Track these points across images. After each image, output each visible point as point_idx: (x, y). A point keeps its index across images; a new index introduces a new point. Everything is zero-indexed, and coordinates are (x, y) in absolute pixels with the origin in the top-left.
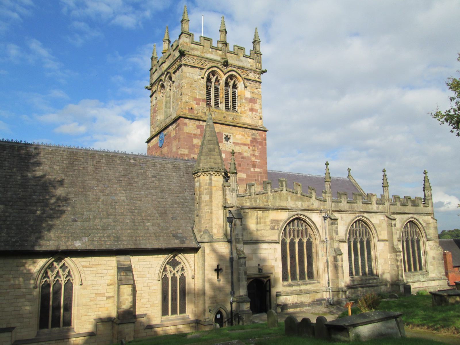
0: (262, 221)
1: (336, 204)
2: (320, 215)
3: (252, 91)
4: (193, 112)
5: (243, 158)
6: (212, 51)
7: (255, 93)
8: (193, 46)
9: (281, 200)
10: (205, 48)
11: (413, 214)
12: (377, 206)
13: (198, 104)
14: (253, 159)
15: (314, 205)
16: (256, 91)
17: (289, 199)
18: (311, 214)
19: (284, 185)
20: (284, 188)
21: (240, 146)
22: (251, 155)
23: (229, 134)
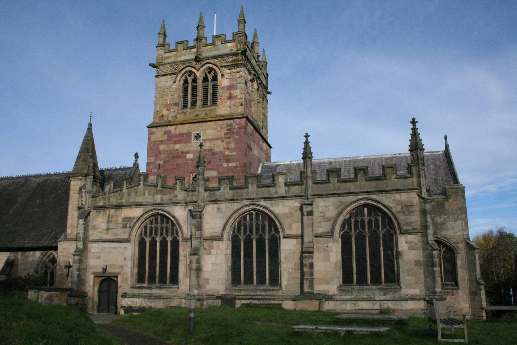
0: (113, 219)
1: (212, 193)
5: (214, 154)
6: (186, 52)
8: (166, 55)
9: (136, 195)
10: (179, 52)
11: (369, 193)
12: (287, 188)
13: (168, 110)
14: (227, 153)
17: (147, 193)
18: (173, 207)
19: (142, 180)
20: (142, 183)
21: (211, 142)
22: (224, 149)
23: (199, 132)
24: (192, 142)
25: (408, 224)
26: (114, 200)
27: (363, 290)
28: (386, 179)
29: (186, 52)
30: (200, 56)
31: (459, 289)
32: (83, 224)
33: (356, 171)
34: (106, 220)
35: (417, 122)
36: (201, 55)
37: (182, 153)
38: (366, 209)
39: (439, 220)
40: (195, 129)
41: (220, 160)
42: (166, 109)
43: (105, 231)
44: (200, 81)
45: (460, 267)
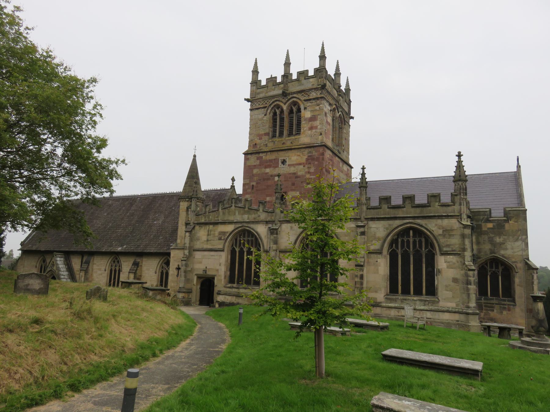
0: (212, 233)
2: (266, 225)
3: (312, 109)
4: (256, 147)
5: (297, 177)
7: (316, 110)
10: (269, 88)
11: (414, 218)
13: (260, 139)
14: (308, 176)
15: (261, 216)
16: (317, 108)
17: (237, 213)
18: (257, 225)
19: (234, 202)
20: (233, 205)
22: (306, 173)
23: (285, 158)
24: (280, 167)
25: (448, 246)
26: (212, 218)
27: (406, 300)
28: (430, 206)
29: (275, 88)
30: (286, 91)
31: (516, 305)
32: (189, 236)
33: (405, 198)
34: (206, 233)
35: (462, 155)
36: (287, 90)
37: (271, 176)
38: (411, 232)
39: (498, 240)
40: (282, 156)
41: (302, 182)
42: (258, 138)
43: (206, 242)
44: (286, 113)
45: (518, 285)
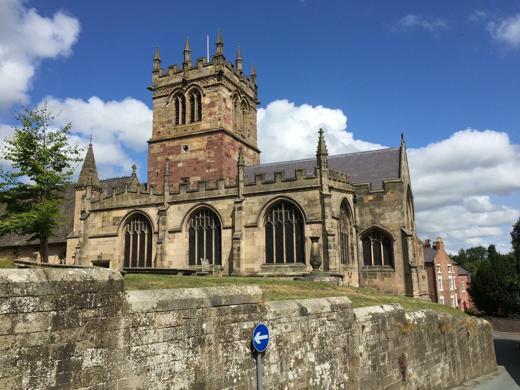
0: (107, 219)
1: (174, 195)
3: (211, 95)
4: (160, 135)
5: (198, 162)
6: (176, 76)
8: (160, 79)
9: (122, 200)
10: (170, 76)
12: (226, 190)
14: (208, 161)
15: (152, 199)
16: (216, 94)
20: (126, 190)
21: (196, 153)
23: (187, 145)
24: (182, 153)
25: (312, 215)
26: (107, 205)
27: (278, 267)
28: (297, 180)
29: (176, 76)
30: (186, 79)
31: (395, 271)
32: (84, 224)
33: (276, 174)
34: (101, 220)
35: (324, 132)
36: (187, 78)
37: (175, 162)
38: (283, 205)
39: (378, 211)
40: (184, 142)
41: (203, 167)
42: (161, 125)
43: (101, 228)
45: (396, 252)
